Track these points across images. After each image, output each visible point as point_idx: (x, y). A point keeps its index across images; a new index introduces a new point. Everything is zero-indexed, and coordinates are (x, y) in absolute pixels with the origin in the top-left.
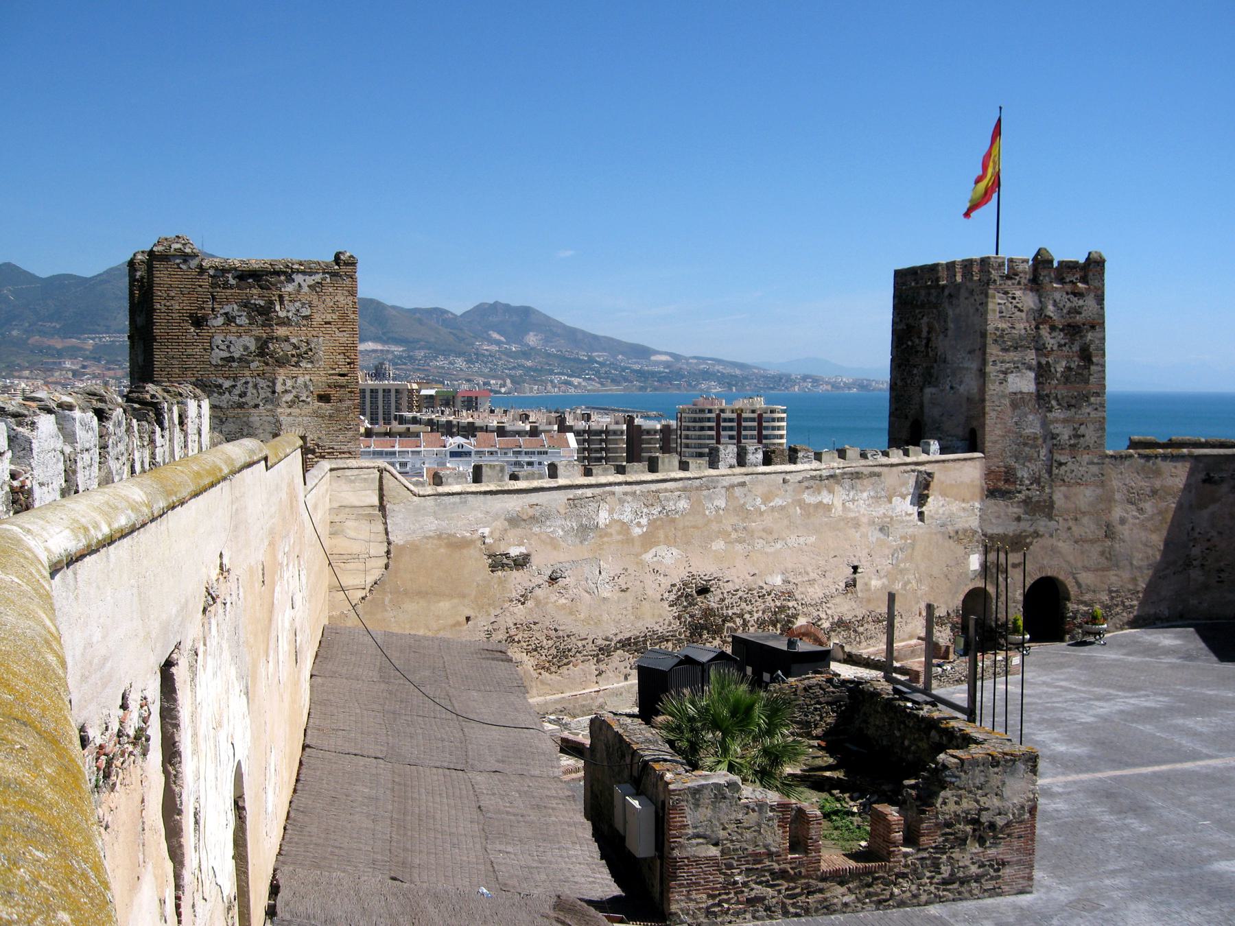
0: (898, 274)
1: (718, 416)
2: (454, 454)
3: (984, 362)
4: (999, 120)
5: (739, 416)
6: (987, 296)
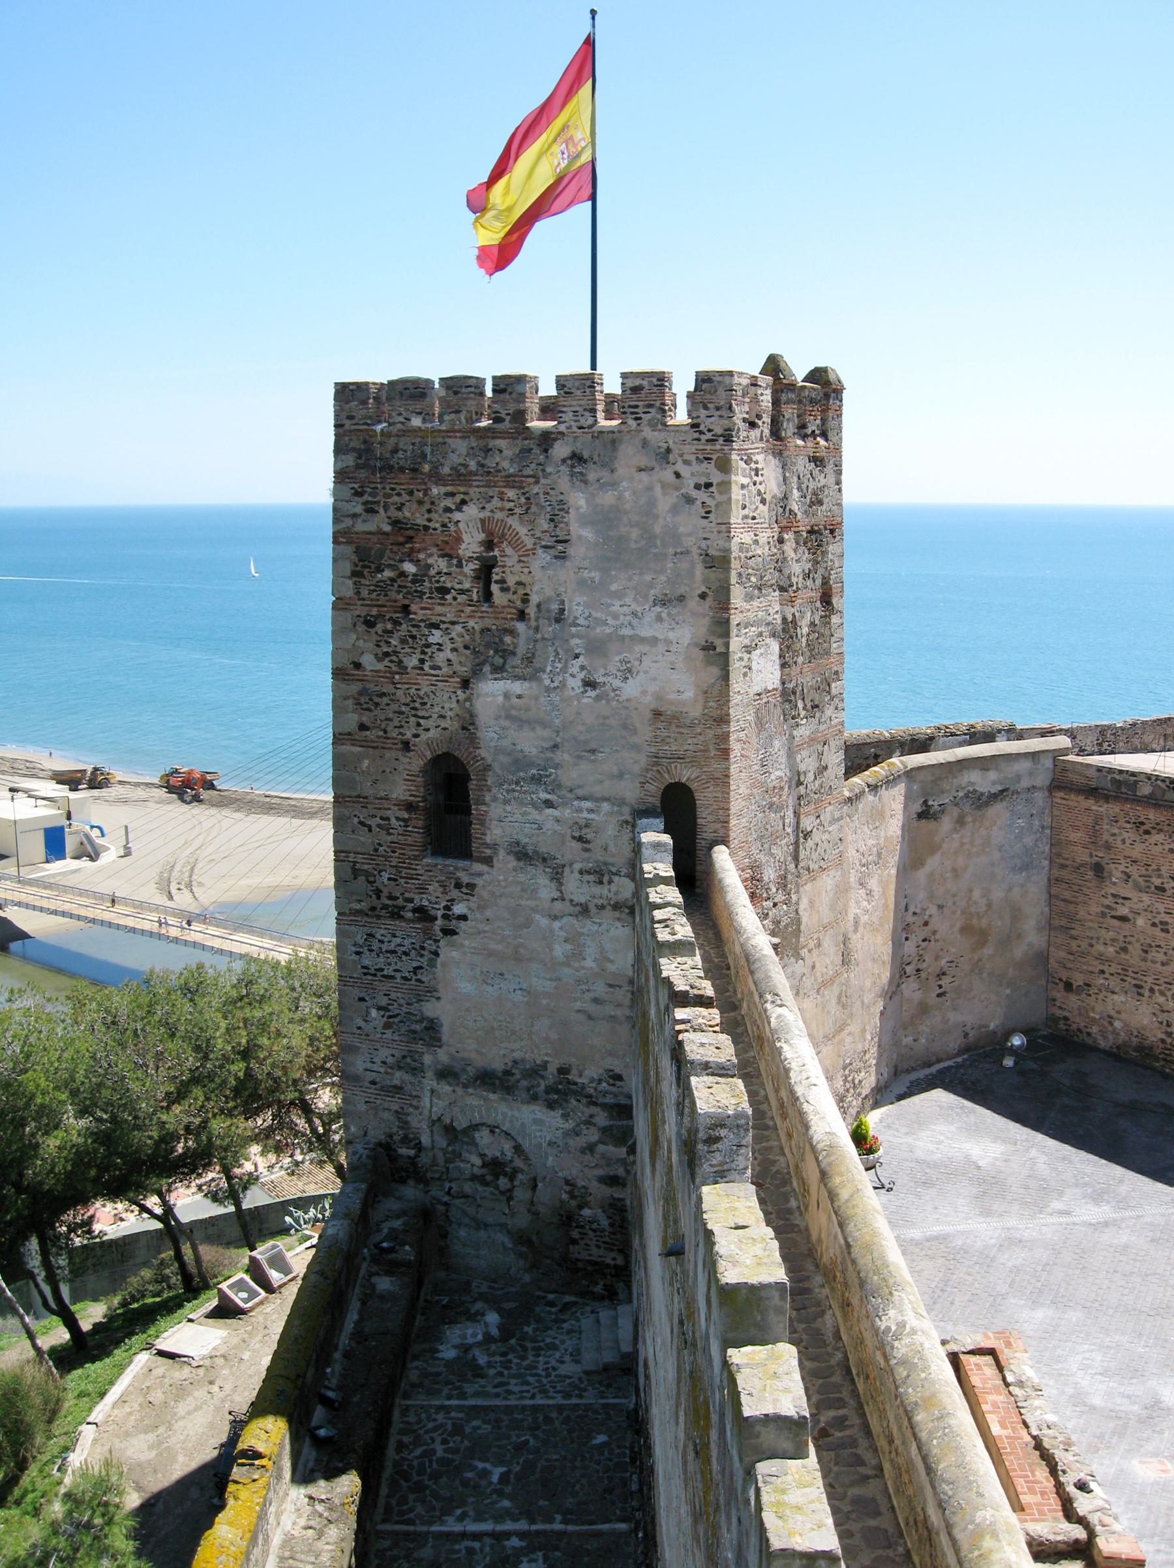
0: (346, 394)
3: (722, 626)
4: (590, 43)
6: (725, 466)
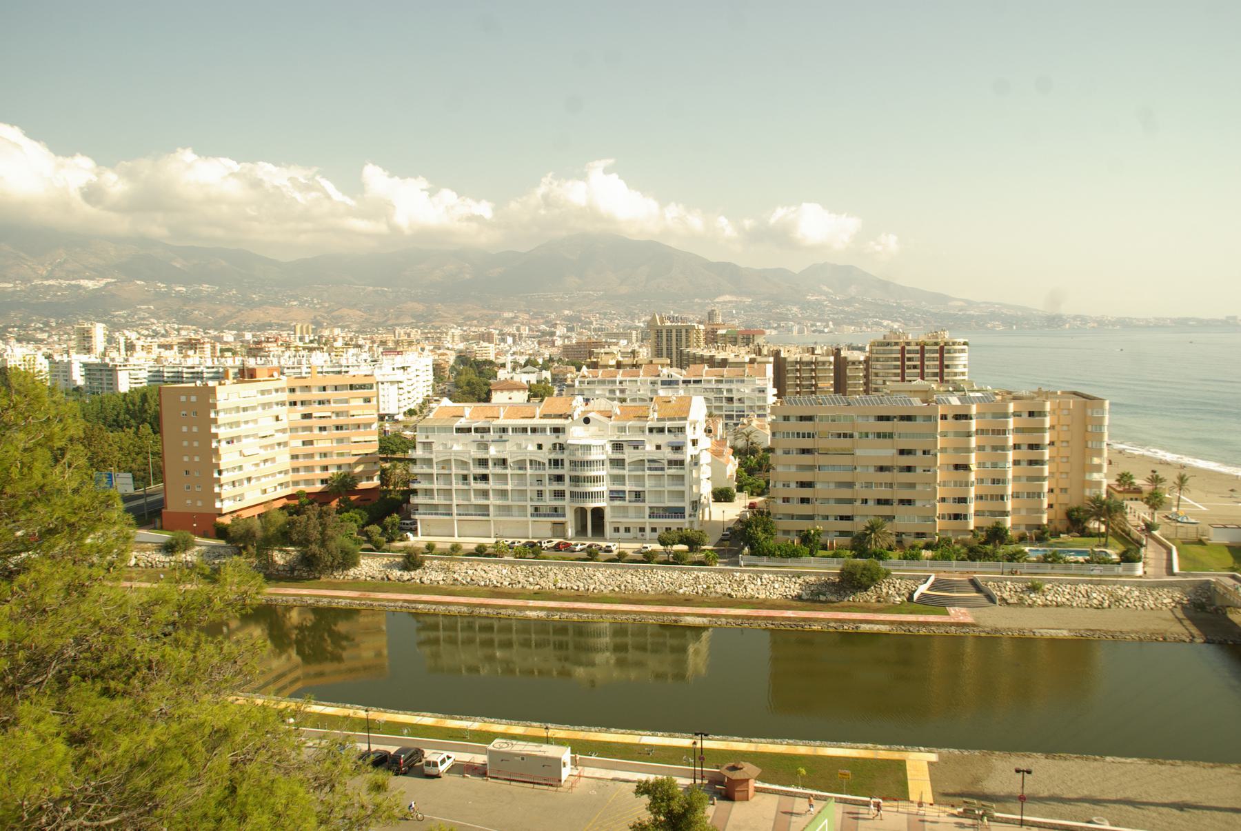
1: (903, 348)
2: (663, 383)
5: (922, 348)
